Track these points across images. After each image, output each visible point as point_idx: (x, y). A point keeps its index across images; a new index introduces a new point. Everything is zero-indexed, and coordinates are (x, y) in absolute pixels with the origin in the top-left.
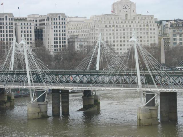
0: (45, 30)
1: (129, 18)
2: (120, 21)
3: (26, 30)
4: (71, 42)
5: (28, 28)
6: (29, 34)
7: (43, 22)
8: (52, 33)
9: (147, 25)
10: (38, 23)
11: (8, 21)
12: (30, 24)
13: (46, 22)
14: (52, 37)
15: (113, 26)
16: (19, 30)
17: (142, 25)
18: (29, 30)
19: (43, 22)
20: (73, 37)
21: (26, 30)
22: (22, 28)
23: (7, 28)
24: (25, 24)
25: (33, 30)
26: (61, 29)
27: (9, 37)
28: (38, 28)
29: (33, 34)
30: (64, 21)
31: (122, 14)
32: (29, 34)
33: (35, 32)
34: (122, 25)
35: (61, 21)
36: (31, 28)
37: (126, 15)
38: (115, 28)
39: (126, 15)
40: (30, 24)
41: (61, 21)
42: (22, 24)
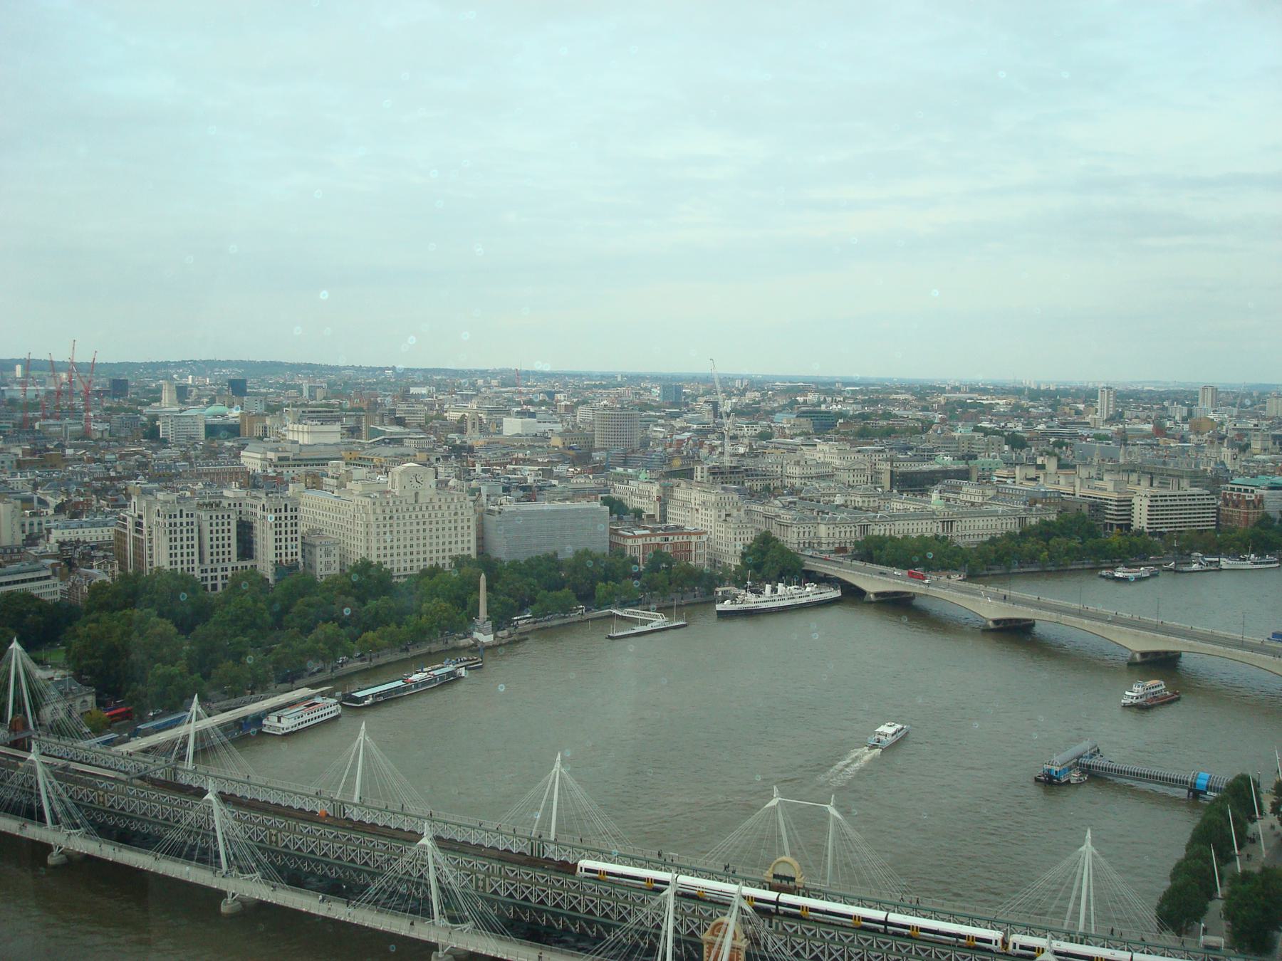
0: (258, 525)
1: (420, 501)
2: (404, 506)
3: (220, 528)
4: (308, 547)
7: (253, 510)
8: (270, 537)
9: (456, 514)
10: (244, 509)
11: (185, 520)
13: (259, 513)
14: (271, 544)
15: (391, 518)
17: (446, 514)
19: (253, 510)
20: (313, 531)
21: (220, 528)
25: (233, 527)
26: (289, 529)
27: (185, 550)
29: (234, 534)
30: (294, 514)
31: (409, 494)
32: (226, 535)
34: (407, 515)
35: (289, 514)
37: (417, 494)
38: (395, 521)
39: (417, 494)
41: (289, 514)
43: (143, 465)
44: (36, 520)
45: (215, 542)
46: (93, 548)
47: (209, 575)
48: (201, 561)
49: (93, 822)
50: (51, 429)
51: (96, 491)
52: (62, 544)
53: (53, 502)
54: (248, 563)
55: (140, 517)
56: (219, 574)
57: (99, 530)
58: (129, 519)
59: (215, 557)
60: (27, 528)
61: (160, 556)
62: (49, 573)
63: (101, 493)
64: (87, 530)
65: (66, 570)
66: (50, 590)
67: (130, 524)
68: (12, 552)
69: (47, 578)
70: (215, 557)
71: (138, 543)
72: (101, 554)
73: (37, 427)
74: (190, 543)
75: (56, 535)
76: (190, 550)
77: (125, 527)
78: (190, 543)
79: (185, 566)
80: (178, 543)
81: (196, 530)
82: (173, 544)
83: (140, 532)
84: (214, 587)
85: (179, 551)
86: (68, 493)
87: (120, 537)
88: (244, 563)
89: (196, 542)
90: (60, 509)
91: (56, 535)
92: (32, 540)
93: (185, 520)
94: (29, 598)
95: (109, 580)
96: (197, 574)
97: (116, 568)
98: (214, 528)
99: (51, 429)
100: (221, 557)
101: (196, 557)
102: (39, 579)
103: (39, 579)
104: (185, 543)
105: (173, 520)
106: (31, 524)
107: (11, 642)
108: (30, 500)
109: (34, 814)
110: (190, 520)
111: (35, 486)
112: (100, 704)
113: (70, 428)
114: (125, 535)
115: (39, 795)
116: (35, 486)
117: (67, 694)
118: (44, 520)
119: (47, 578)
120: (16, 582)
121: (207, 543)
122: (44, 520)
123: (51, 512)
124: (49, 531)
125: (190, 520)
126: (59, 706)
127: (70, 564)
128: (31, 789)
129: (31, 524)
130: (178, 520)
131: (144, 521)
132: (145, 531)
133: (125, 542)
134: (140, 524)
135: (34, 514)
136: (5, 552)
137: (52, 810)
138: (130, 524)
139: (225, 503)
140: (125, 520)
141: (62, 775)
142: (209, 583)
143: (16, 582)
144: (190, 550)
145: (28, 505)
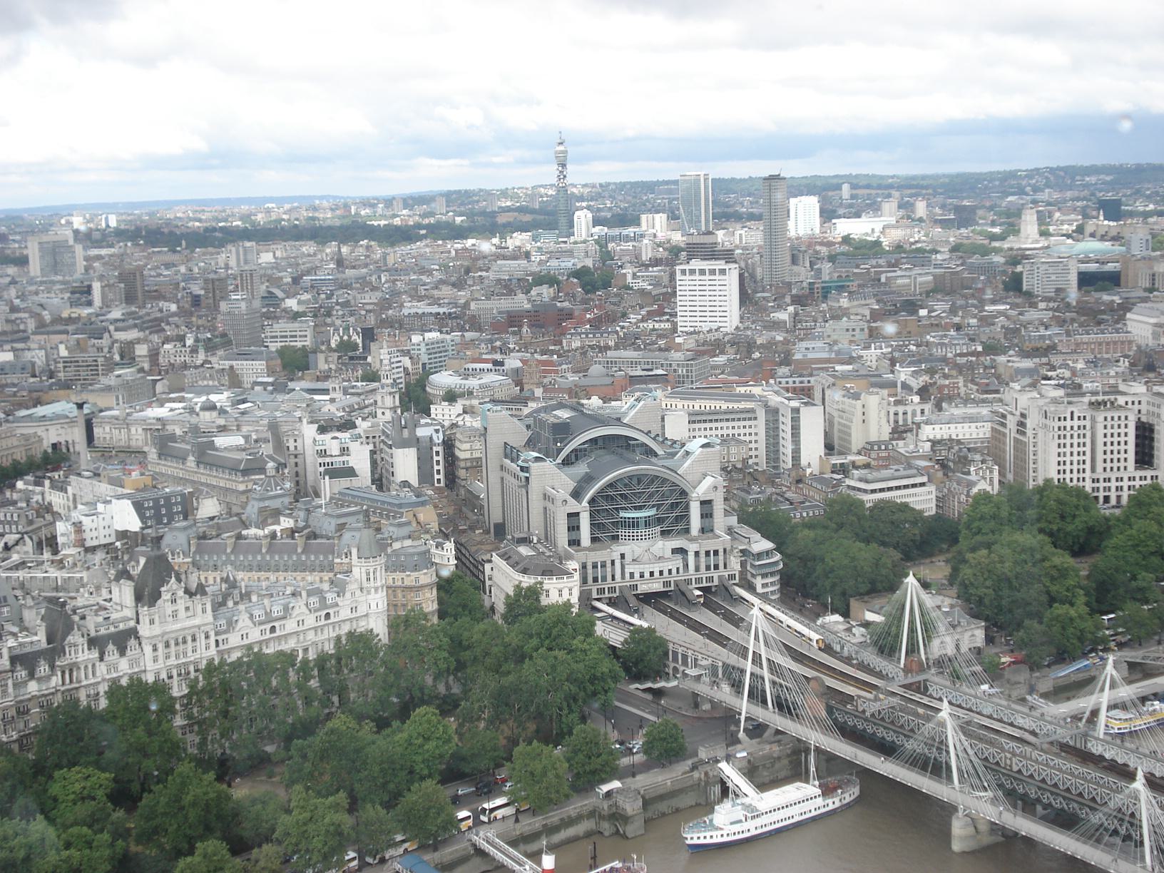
3: (1116, 431)
5: (1119, 426)
6: (1122, 447)
10: (1144, 407)
11: (1076, 423)
12: (1126, 418)
16: (1100, 431)
18: (1122, 430)
21: (1116, 431)
22: (1105, 427)
23: (1072, 436)
24: (1112, 418)
28: (1144, 419)
33: (1137, 428)
36: (1126, 426)
40: (1126, 418)
42: (1106, 419)
43: (1011, 333)
44: (901, 409)
45: (1109, 448)
46: (969, 449)
47: (1102, 485)
48: (1093, 470)
49: (1001, 786)
50: (899, 281)
51: (960, 369)
52: (935, 443)
53: (916, 384)
54: (1149, 473)
55: (1023, 415)
56: (1113, 484)
57: (973, 425)
58: (1009, 417)
59: (1109, 465)
60: (892, 417)
61: (1049, 464)
62: (925, 479)
63: (966, 370)
64: (959, 426)
65: (940, 474)
66: (924, 500)
67: (1011, 422)
68: (880, 449)
69: (923, 484)
70: (1109, 465)
71: (1020, 447)
72: (978, 457)
73: (883, 280)
74: (1081, 449)
75: (928, 432)
76: (1082, 458)
77: (1004, 425)
78: (1081, 449)
79: (1075, 476)
80: (1068, 450)
81: (1089, 434)
82: (1062, 450)
83: (1024, 433)
84: (1107, 499)
85: (1068, 459)
86: (931, 372)
87: (998, 436)
88: (1143, 473)
89: (1088, 449)
90: (924, 392)
91: (928, 432)
92: (899, 432)
93: (1076, 423)
94: (905, 507)
95: (989, 488)
96: (1088, 486)
97: (996, 473)
98: (1109, 431)
99: (899, 281)
100: (1115, 465)
101: (1088, 466)
102: (914, 486)
103: (914, 486)
104: (1075, 449)
105: (1062, 423)
106: (896, 414)
107: (907, 575)
108: (894, 385)
109: (938, 769)
110: (1082, 423)
111: (893, 362)
112: (989, 640)
113: (920, 279)
114: (1004, 435)
115: (948, 752)
116: (893, 362)
117: (954, 627)
118: (909, 409)
119: (923, 484)
120: (890, 489)
121: (1100, 448)
122: (909, 409)
123: (916, 399)
124: (918, 426)
125: (1082, 423)
126: (948, 639)
127: (943, 465)
128: (942, 745)
129: (896, 414)
130: (1068, 423)
131: (1029, 422)
132: (1029, 432)
133: (1004, 444)
134: (1022, 424)
135: (897, 403)
136: (872, 449)
137: (959, 769)
138: (1011, 422)
139: (1121, 400)
140: (1004, 416)
141: (965, 728)
142: (1101, 495)
143: (890, 489)
144: (1082, 458)
145: (892, 391)
